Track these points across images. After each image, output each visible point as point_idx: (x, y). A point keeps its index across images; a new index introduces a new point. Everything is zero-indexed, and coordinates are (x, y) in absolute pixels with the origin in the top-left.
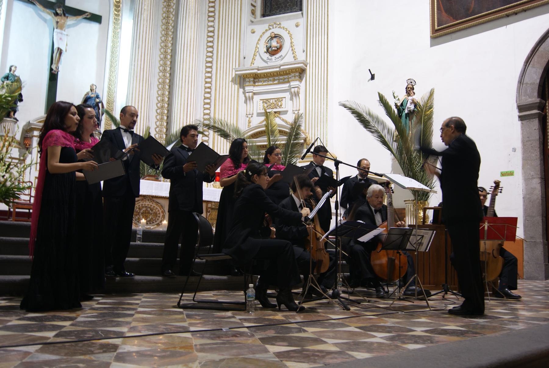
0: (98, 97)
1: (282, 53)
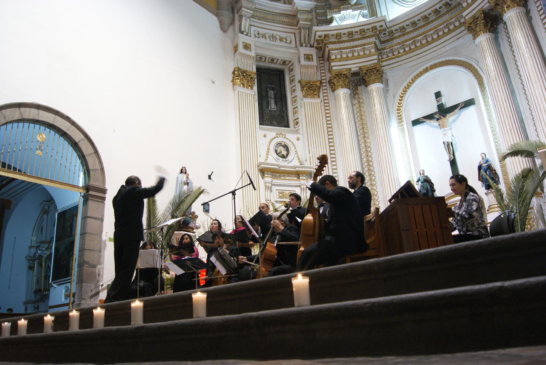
0: (487, 161)
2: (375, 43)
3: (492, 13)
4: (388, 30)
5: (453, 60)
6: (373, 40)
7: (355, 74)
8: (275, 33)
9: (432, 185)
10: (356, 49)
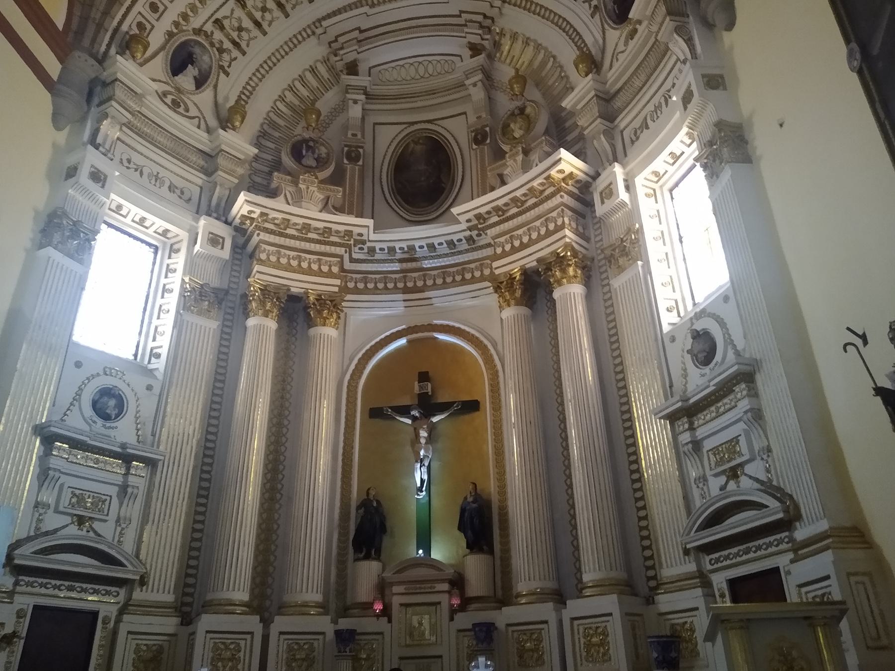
1: (718, 357)
2: (341, 257)
3: (536, 278)
4: (369, 244)
5: (459, 328)
6: (340, 251)
7: (294, 299)
10: (308, 256)
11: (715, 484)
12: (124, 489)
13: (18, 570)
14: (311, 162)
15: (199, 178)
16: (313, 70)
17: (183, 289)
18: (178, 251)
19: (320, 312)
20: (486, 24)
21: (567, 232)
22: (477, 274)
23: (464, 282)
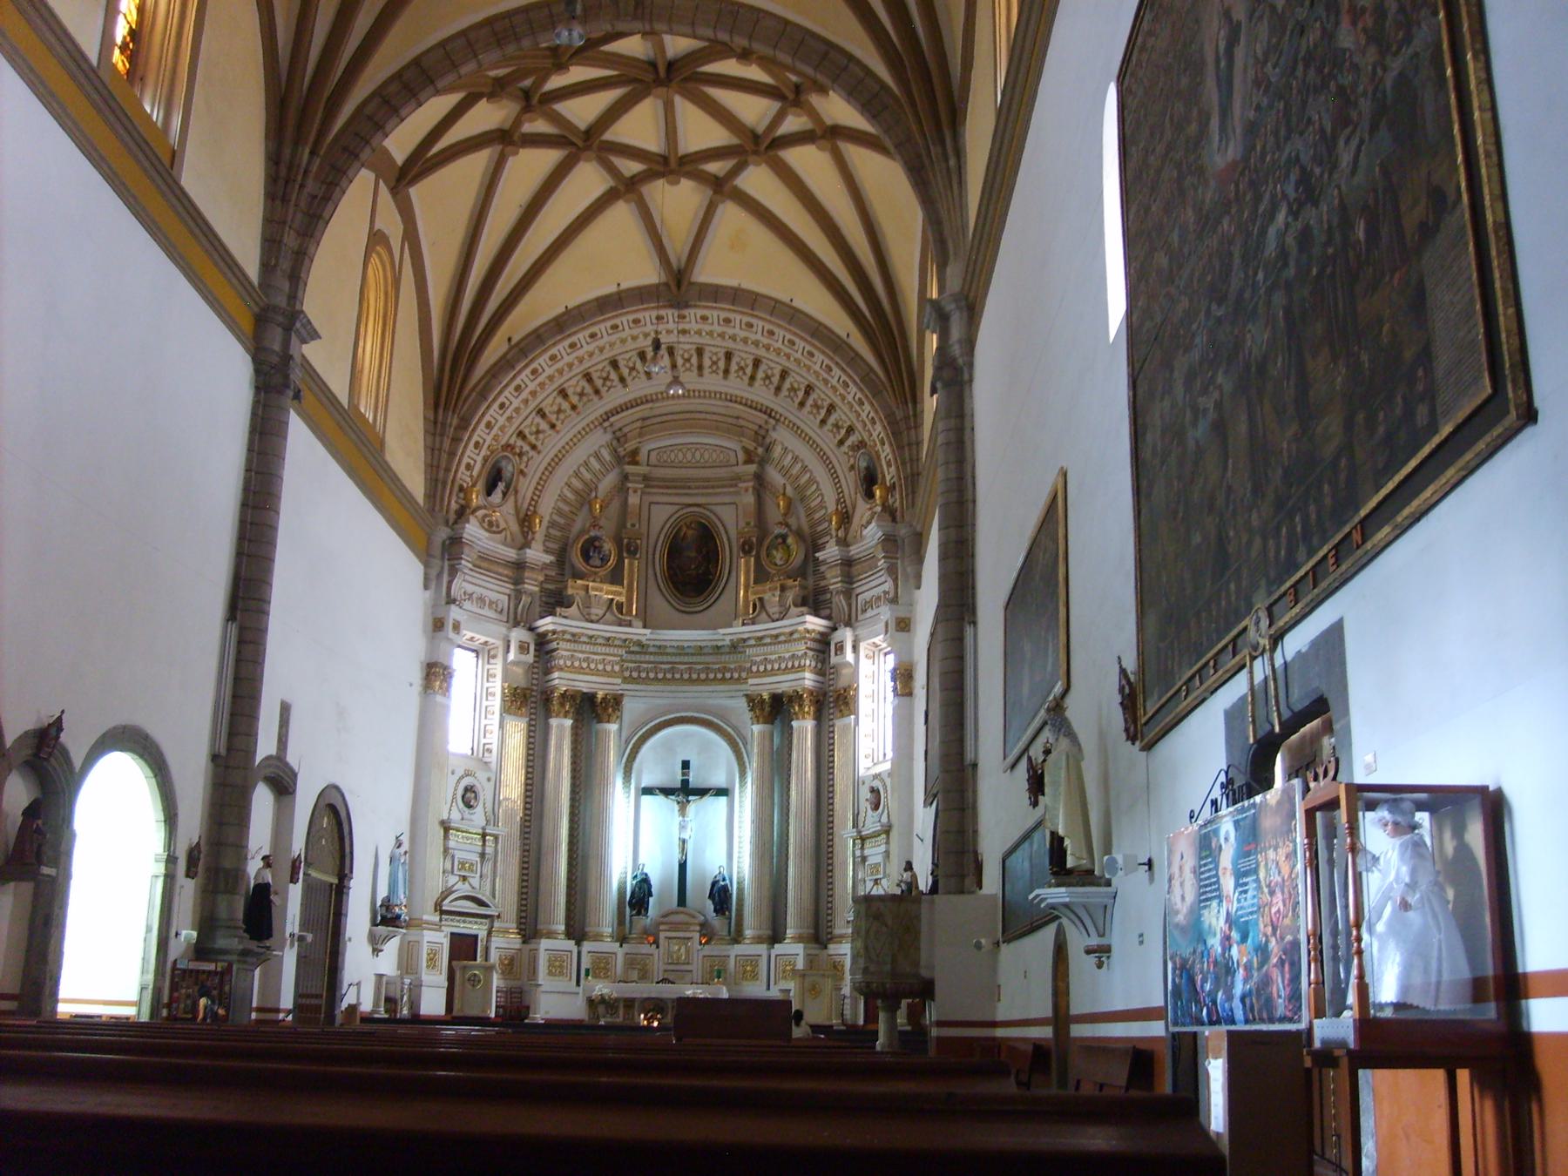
8: (485, 593)
9: (650, 886)
11: (869, 884)
12: (483, 855)
13: (443, 912)
14: (598, 562)
15: (508, 588)
16: (597, 456)
17: (503, 693)
18: (494, 657)
19: (605, 709)
20: (761, 436)
21: (808, 675)
22: (736, 675)
23: (723, 680)
